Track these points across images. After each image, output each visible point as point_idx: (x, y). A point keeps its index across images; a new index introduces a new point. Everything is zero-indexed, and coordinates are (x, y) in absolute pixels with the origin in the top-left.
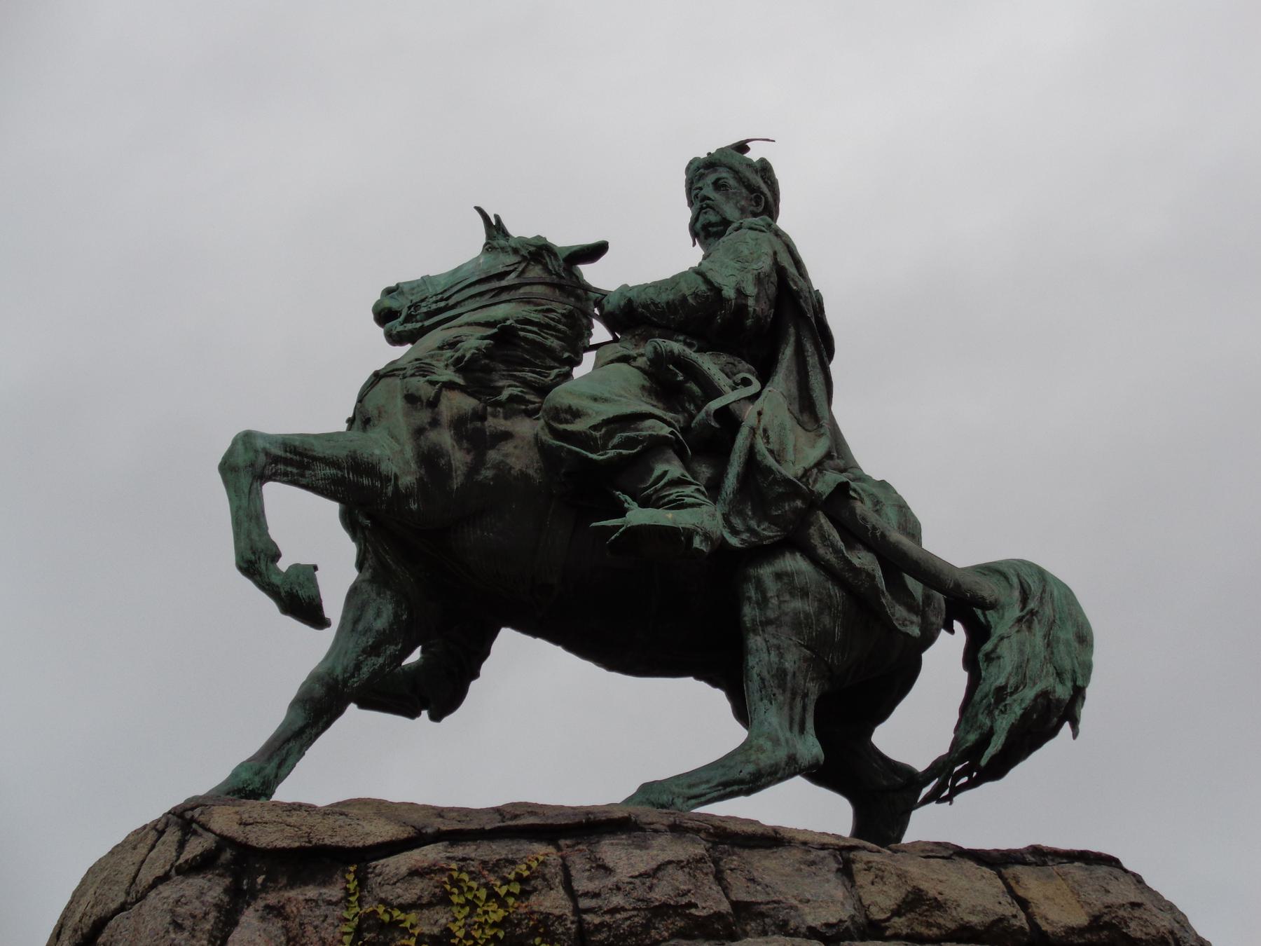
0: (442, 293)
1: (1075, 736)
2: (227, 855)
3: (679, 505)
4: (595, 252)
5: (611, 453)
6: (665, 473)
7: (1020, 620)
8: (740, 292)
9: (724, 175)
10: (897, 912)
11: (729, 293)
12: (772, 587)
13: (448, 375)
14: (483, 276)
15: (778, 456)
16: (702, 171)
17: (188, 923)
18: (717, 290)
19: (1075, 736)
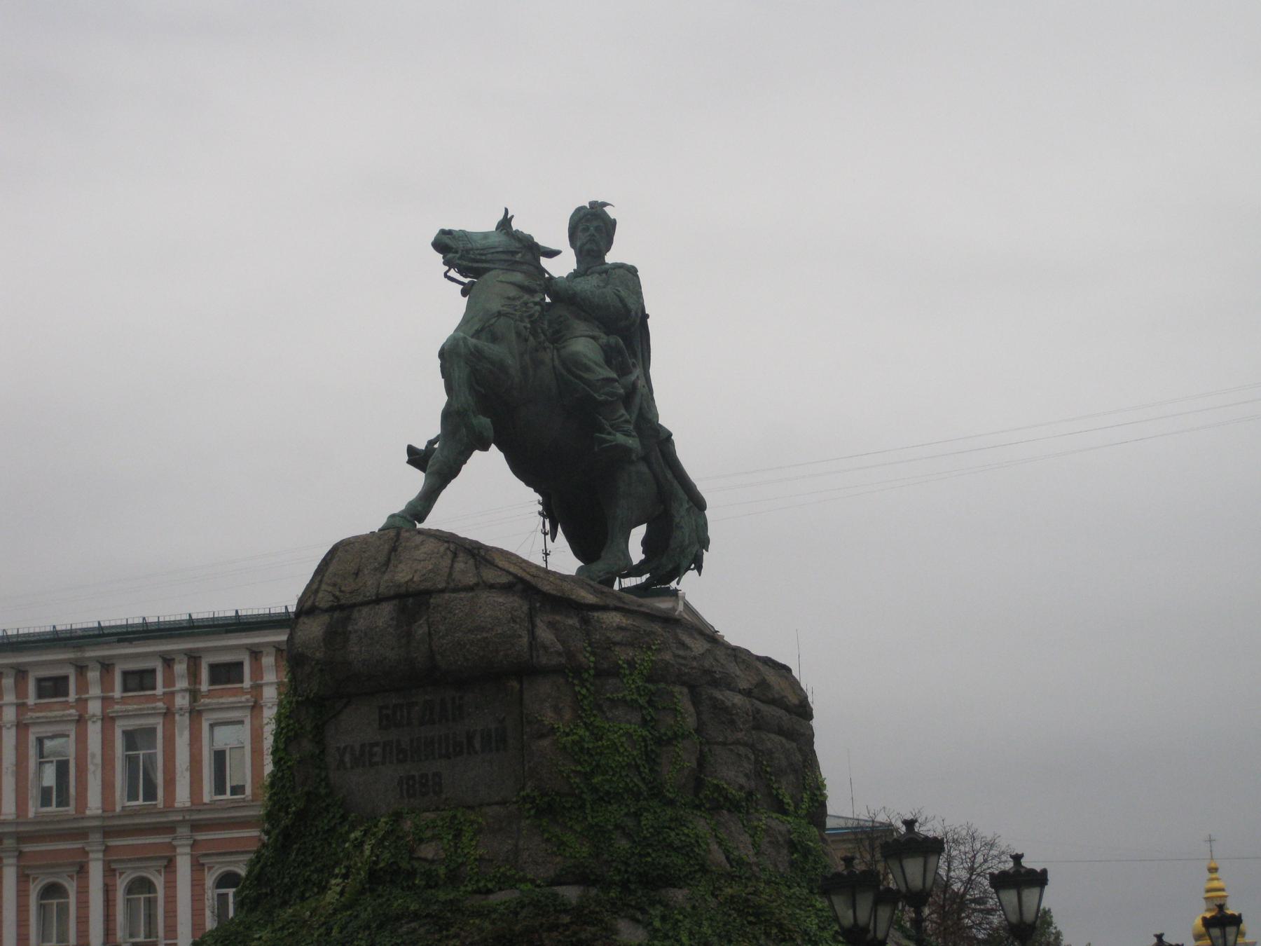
0: (482, 249)
1: (700, 575)
2: (519, 587)
3: (627, 434)
4: (552, 254)
5: (603, 398)
6: (623, 415)
7: (687, 509)
8: (636, 314)
9: (602, 224)
10: (757, 686)
11: (633, 313)
13: (529, 325)
14: (505, 250)
16: (589, 216)
17: (518, 620)
18: (628, 311)
19: (700, 575)
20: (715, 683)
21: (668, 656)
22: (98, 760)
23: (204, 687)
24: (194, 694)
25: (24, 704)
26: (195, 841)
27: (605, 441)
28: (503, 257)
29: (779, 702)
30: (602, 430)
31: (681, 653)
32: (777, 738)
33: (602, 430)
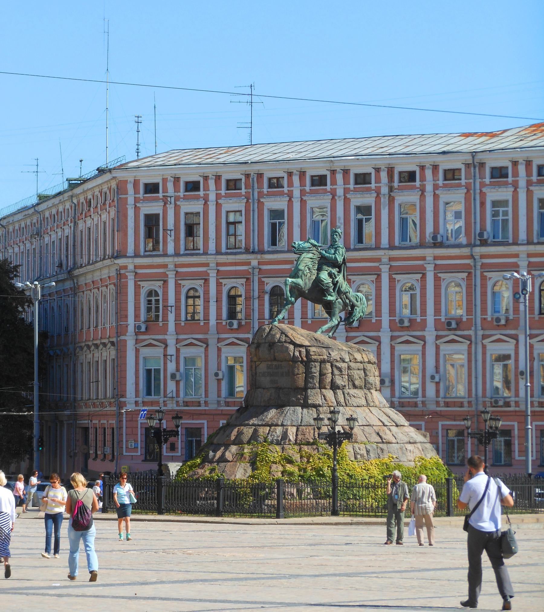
3: (332, 296)
12: (337, 303)
13: (308, 271)
15: (342, 287)
20: (337, 361)
21: (326, 357)
22: (343, 222)
23: (396, 184)
24: (391, 189)
25: (304, 190)
26: (391, 266)
27: (325, 299)
28: (308, 249)
29: (361, 362)
30: (326, 296)
31: (329, 356)
32: (355, 371)
33: (326, 296)
